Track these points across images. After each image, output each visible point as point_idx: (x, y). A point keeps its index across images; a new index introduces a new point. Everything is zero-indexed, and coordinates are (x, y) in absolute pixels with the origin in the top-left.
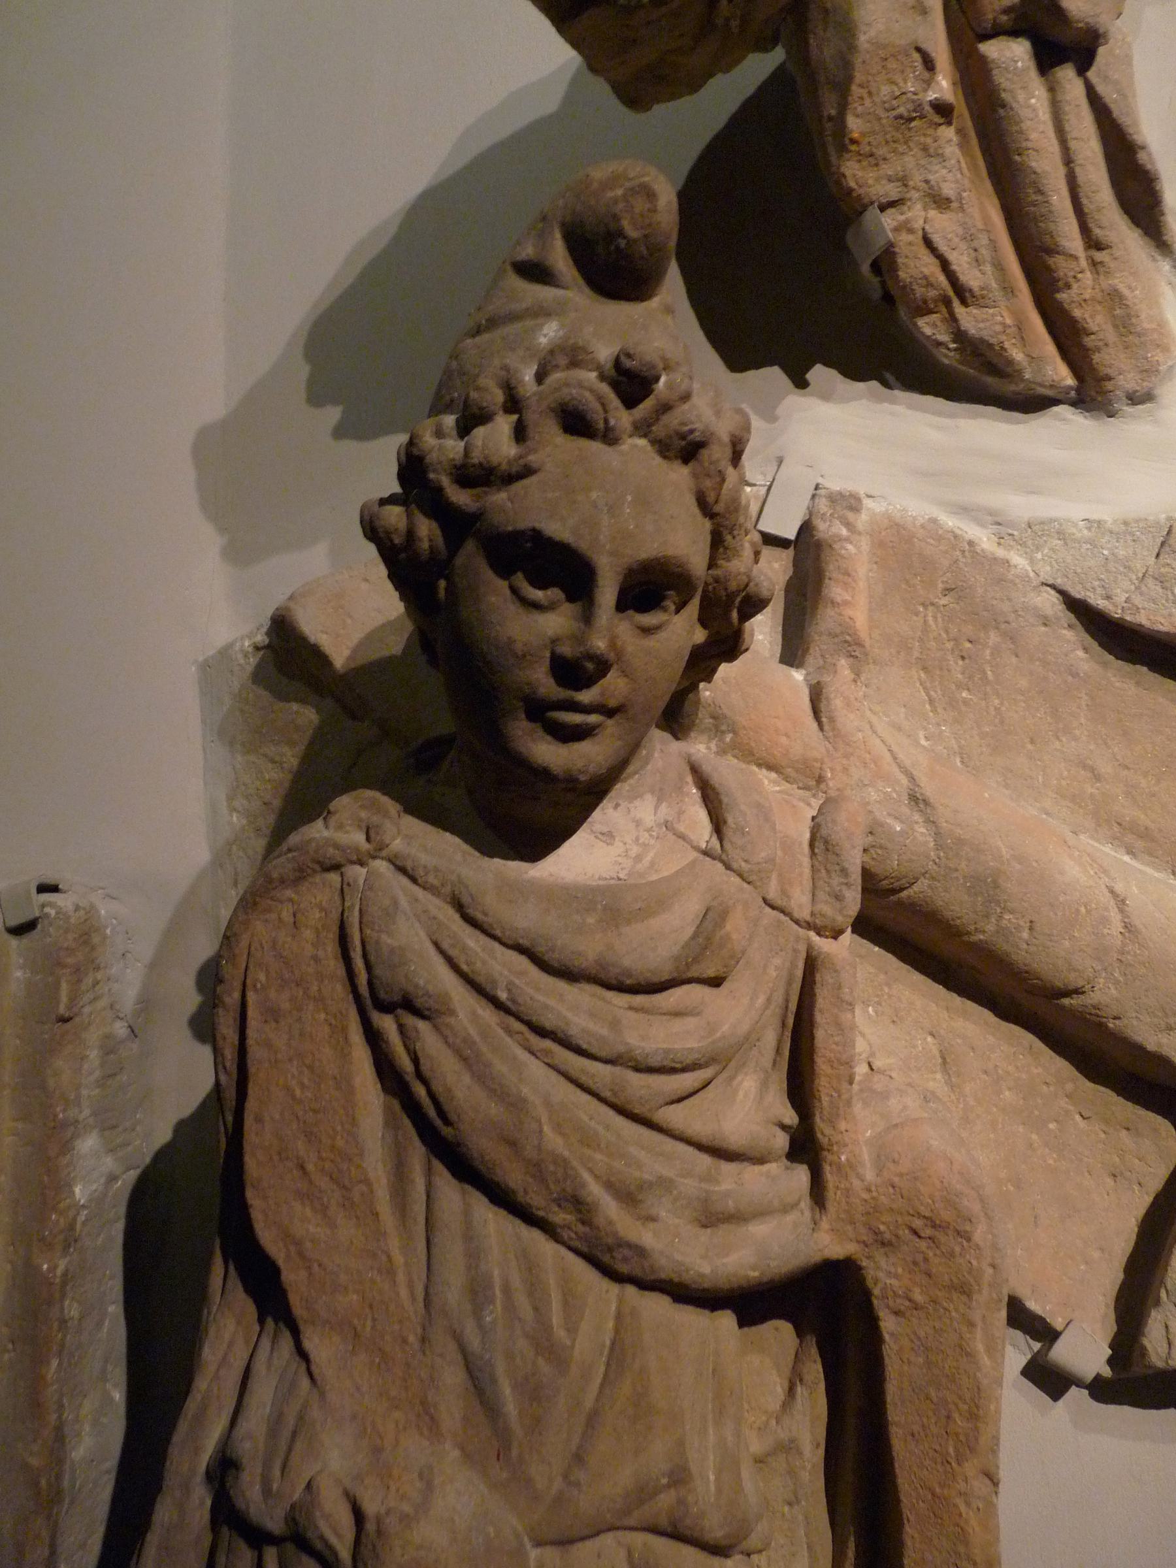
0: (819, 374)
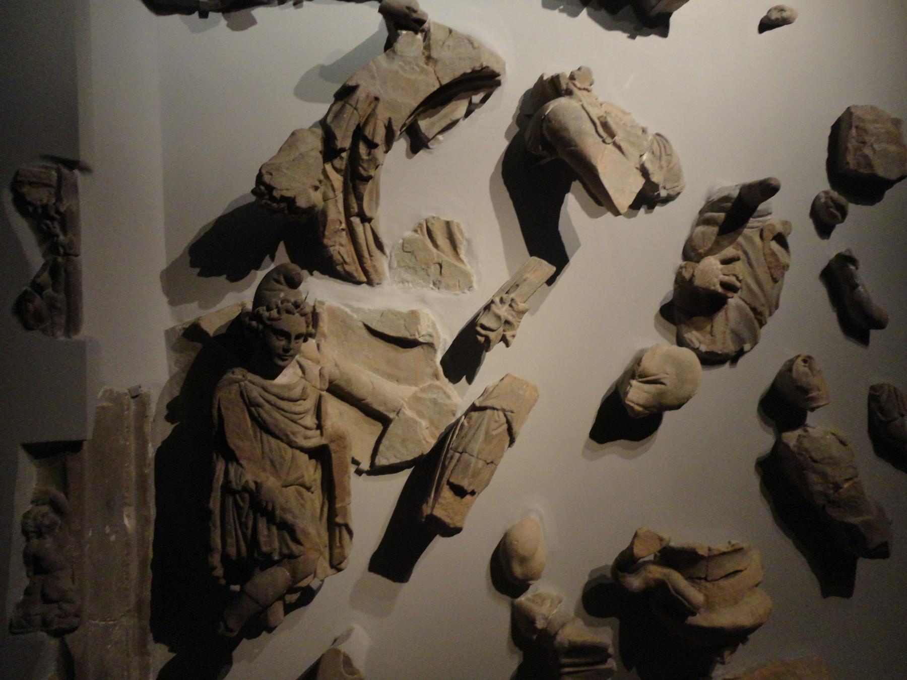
0: (316, 273)
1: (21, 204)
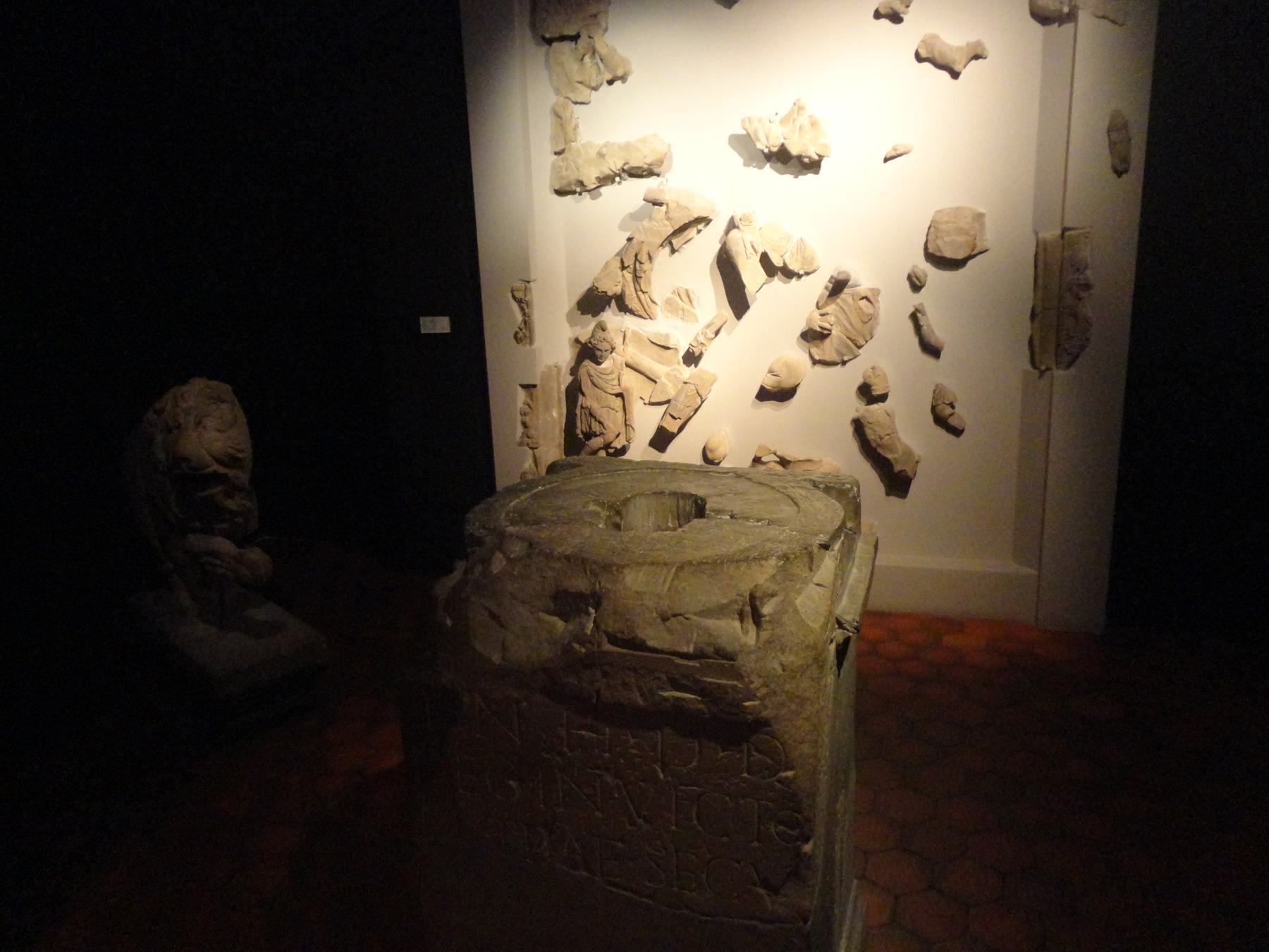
1: (514, 297)
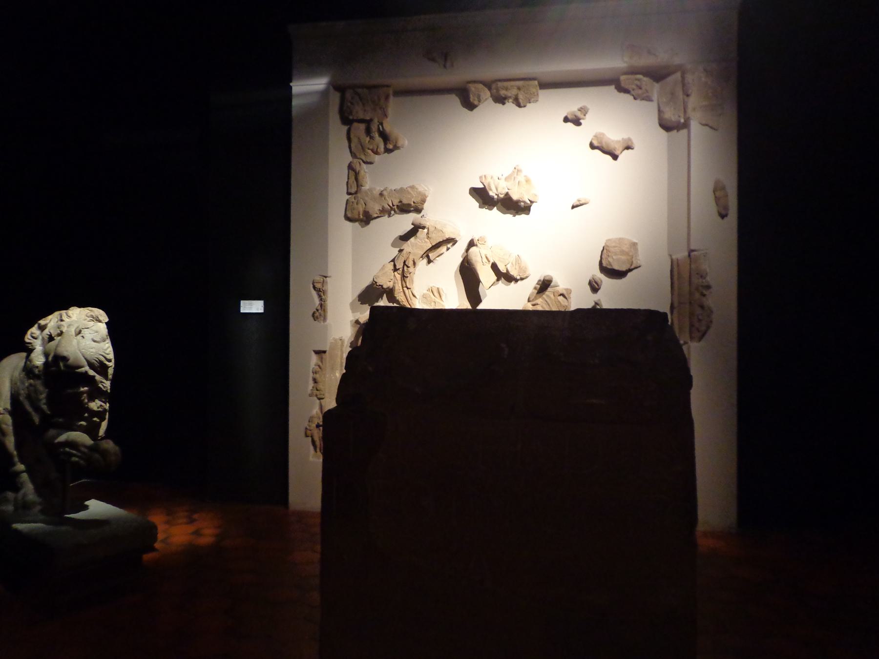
1: (314, 287)
